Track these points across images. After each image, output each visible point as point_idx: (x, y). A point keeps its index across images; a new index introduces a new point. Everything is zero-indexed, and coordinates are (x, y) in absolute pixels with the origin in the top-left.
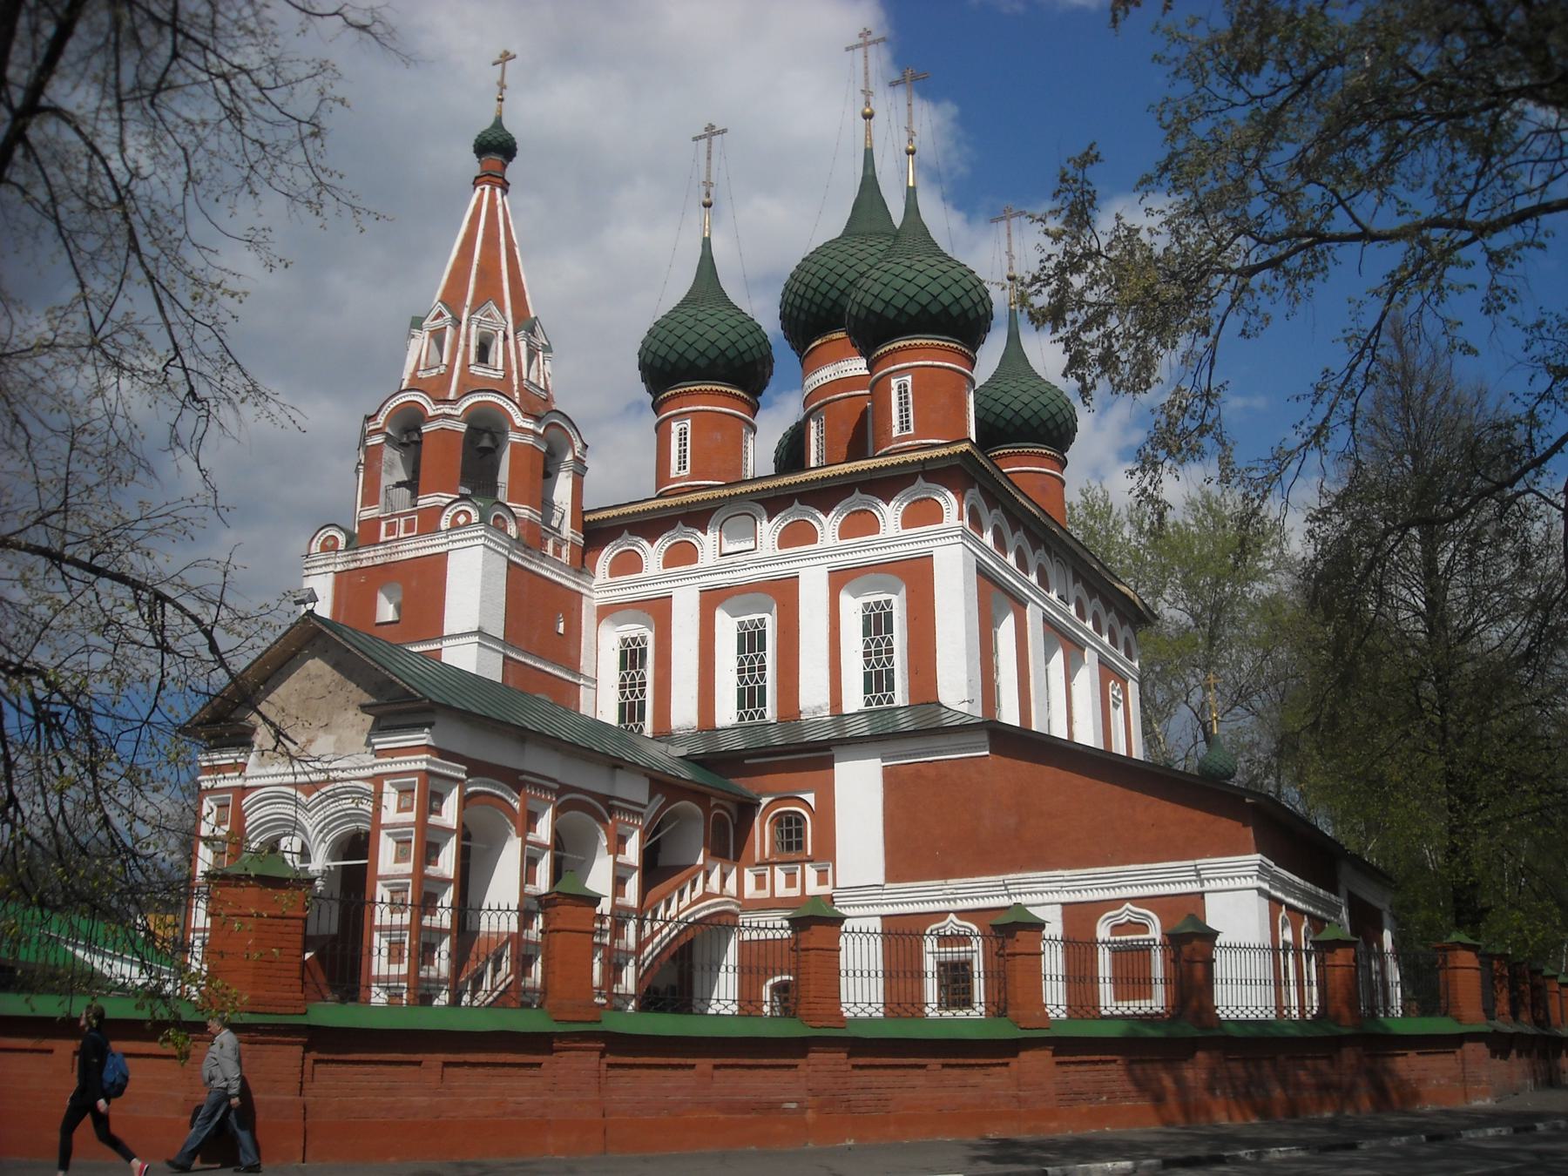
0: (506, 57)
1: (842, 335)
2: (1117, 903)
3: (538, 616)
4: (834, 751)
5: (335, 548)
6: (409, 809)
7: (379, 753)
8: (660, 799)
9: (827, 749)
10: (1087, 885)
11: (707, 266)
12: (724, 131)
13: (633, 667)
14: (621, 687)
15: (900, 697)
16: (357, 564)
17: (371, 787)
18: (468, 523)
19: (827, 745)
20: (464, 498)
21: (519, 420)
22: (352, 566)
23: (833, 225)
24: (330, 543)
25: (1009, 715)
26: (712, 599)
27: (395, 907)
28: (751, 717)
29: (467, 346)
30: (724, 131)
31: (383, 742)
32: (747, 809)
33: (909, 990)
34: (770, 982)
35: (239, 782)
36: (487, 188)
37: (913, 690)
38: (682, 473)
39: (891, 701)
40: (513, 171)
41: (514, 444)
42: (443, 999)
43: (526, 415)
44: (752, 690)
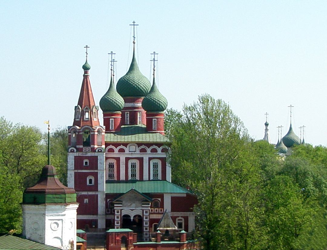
17: (142, 211)
26: (127, 159)
35: (121, 209)
39: (157, 178)
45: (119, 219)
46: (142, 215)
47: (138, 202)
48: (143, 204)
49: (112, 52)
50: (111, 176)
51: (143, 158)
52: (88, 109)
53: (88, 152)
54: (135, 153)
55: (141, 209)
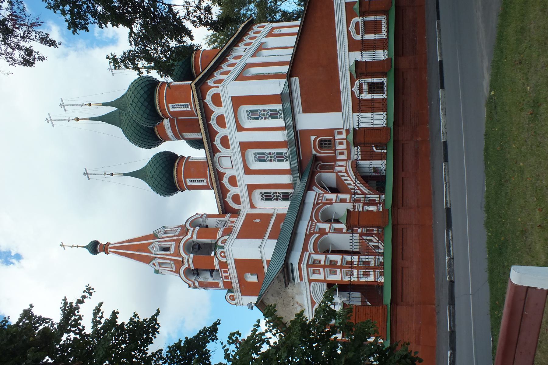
0: (62, 245)
1: (155, 127)
2: (349, 33)
3: (253, 229)
4: (297, 130)
5: (233, 296)
6: (319, 270)
7: (301, 280)
8: (314, 188)
9: (297, 132)
10: (342, 43)
11: (134, 174)
12: (86, 169)
13: (270, 196)
14: (277, 200)
15: (279, 107)
16: (239, 289)
17: (312, 283)
18: (224, 252)
19: (296, 132)
20: (215, 254)
21: (189, 236)
22: (239, 290)
23: (118, 131)
24: (232, 298)
25: (285, 69)
26: (248, 171)
27: (351, 275)
28: (287, 157)
29: (164, 255)
30: (86, 169)
32: (316, 159)
33: (378, 104)
34: (375, 150)
36: (109, 250)
37: (276, 103)
38: (205, 181)
39: (280, 110)
40: (103, 242)
41: (197, 238)
42: (381, 259)
43: (187, 234)
44: (277, 157)
48: (294, 280)
54: (232, 157)
55: (308, 284)
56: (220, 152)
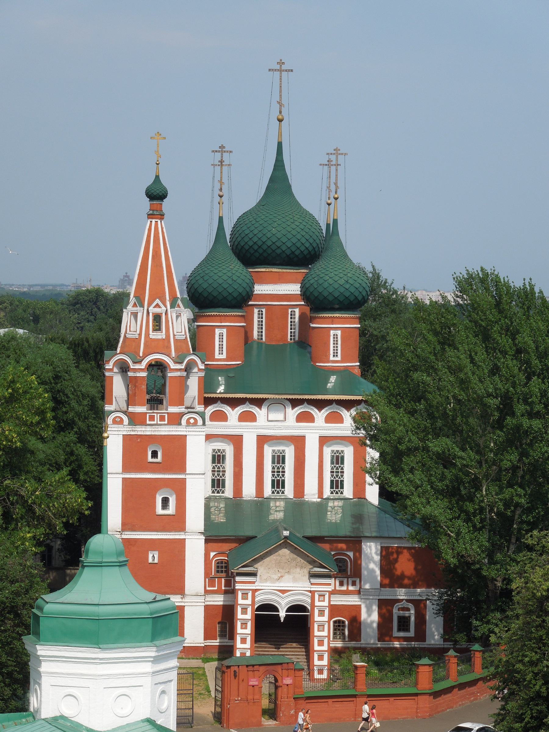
4: (362, 539)
5: (121, 422)
7: (312, 584)
13: (219, 462)
17: (310, 594)
26: (262, 440)
31: (314, 581)
39: (342, 493)
44: (278, 481)
45: (249, 616)
46: (309, 608)
47: (298, 570)
49: (222, 147)
50: (218, 484)
51: (304, 437)
52: (160, 307)
53: (157, 425)
55: (309, 589)
56: (292, 409)
